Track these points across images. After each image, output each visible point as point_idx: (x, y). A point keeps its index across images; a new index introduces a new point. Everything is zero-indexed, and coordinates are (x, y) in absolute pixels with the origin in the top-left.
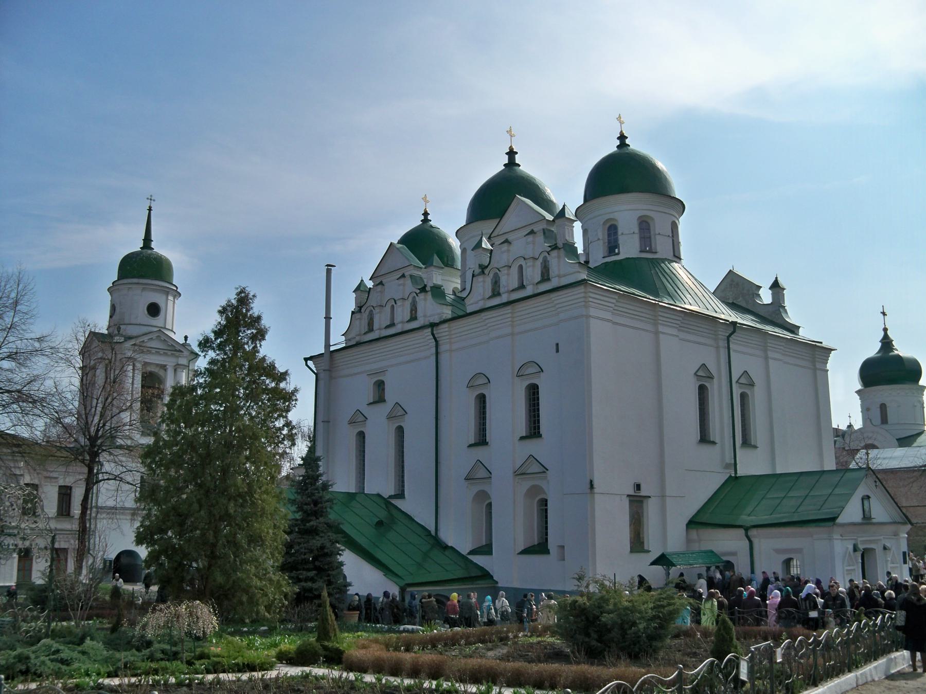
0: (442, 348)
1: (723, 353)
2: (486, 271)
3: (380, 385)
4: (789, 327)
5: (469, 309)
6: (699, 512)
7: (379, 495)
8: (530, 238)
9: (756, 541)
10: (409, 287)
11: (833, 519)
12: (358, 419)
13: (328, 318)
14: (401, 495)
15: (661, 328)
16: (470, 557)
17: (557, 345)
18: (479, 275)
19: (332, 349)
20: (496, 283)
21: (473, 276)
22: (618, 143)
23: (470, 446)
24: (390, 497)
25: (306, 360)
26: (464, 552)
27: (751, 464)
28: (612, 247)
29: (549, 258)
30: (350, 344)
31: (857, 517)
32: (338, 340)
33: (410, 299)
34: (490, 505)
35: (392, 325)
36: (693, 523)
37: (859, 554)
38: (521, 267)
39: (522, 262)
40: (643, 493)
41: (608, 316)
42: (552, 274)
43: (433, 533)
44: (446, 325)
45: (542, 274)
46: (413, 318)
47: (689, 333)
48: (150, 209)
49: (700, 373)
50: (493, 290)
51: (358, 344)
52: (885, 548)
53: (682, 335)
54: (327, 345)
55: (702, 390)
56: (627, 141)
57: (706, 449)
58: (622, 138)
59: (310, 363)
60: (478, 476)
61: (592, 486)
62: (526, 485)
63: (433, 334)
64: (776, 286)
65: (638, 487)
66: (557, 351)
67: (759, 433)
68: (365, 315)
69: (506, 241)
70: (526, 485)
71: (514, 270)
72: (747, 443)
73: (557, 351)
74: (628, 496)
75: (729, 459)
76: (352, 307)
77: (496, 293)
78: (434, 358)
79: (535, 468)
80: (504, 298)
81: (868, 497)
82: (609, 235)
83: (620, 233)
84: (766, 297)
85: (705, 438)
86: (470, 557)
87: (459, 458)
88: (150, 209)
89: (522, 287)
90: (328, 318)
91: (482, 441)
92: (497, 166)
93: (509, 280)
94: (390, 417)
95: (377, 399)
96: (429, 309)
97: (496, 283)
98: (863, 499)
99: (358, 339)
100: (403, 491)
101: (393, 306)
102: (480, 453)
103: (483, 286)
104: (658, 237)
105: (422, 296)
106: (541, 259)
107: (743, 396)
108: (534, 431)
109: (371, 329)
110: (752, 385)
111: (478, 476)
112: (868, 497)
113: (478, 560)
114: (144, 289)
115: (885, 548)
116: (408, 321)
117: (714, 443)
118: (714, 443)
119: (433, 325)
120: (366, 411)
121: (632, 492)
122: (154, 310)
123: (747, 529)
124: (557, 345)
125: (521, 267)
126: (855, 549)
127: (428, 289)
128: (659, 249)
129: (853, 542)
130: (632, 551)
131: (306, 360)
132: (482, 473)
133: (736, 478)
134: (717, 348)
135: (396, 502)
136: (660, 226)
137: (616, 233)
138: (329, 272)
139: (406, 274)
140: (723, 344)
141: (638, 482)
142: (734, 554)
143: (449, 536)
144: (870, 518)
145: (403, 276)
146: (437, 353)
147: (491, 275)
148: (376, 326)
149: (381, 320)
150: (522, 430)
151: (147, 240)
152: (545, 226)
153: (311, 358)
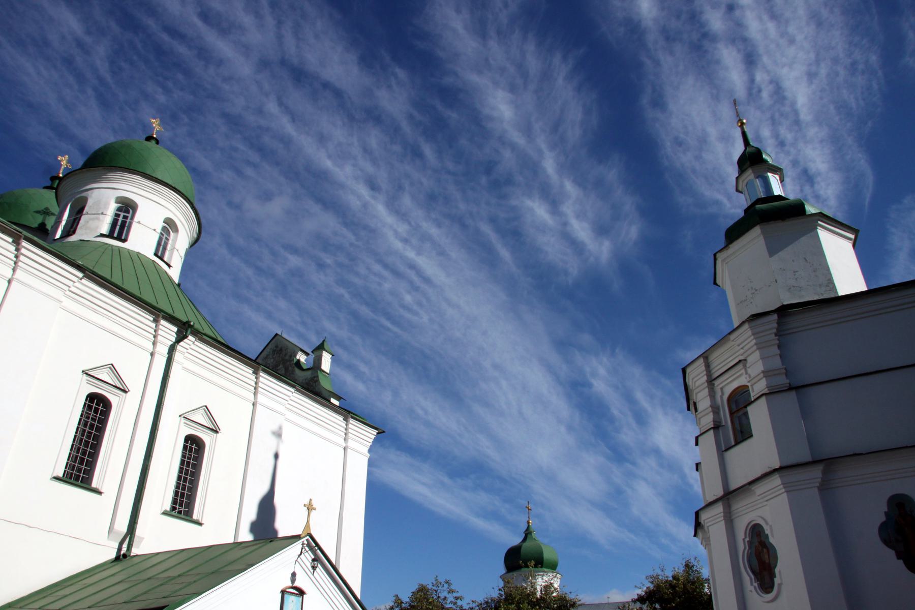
4: (325, 394)
28: (71, 229)
47: (88, 307)
49: (105, 375)
53: (67, 303)
75: (122, 526)
98: (283, 592)
112: (301, 593)
117: (97, 492)
118: (97, 492)
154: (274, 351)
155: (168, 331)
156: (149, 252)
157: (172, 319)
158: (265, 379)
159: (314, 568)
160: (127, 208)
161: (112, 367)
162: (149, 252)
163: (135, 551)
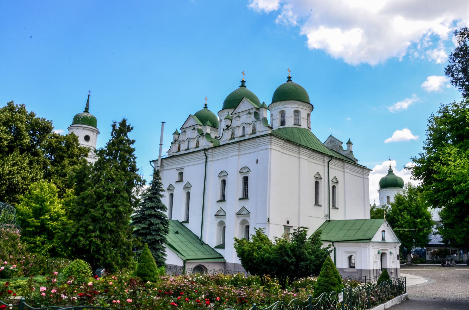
0: (208, 160)
1: (326, 168)
2: (229, 128)
3: (181, 174)
5: (221, 144)
7: (177, 221)
8: (249, 115)
10: (196, 133)
11: (370, 239)
12: (171, 188)
13: (161, 145)
14: (187, 222)
15: (301, 156)
16: (215, 249)
17: (257, 160)
18: (226, 129)
19: (162, 158)
20: (233, 133)
21: (224, 130)
22: (287, 80)
23: (218, 201)
24: (183, 222)
25: (150, 162)
26: (213, 247)
27: (336, 216)
28: (283, 123)
29: (256, 124)
30: (170, 156)
31: (380, 240)
32: (165, 154)
33: (196, 138)
34: (225, 227)
35: (188, 149)
37: (380, 255)
38: (244, 127)
39: (245, 125)
40: (290, 225)
41: (279, 149)
42: (257, 130)
43: (200, 238)
44: (211, 150)
45: (253, 131)
46: (197, 147)
48: (89, 96)
49: (317, 176)
50: (232, 137)
51: (173, 156)
52: (390, 253)
54: (160, 156)
55: (317, 183)
56: (291, 79)
57: (317, 208)
58: (289, 78)
59: (152, 163)
60: (220, 215)
61: (268, 220)
62: (241, 219)
63: (205, 153)
64: (349, 143)
65: (288, 222)
66: (257, 163)
67: (339, 203)
68: (177, 145)
69: (239, 116)
70: (241, 219)
71: (241, 129)
72: (334, 207)
73: (257, 163)
75: (327, 213)
76: (172, 140)
77: (233, 138)
78: (205, 163)
79: (245, 212)
80: (236, 140)
81: (384, 231)
82: (281, 117)
83: (286, 116)
84: (345, 147)
85: (317, 203)
86: (215, 249)
87: (212, 207)
88: (89, 96)
89: (244, 135)
90: (161, 145)
91: (223, 200)
92: (236, 86)
93: (238, 133)
94: (185, 188)
95: (179, 180)
96: (204, 143)
97: (233, 133)
99: (173, 154)
100: (188, 220)
101: (189, 141)
102: (222, 205)
103: (228, 135)
104: (302, 119)
105: (201, 137)
106: (252, 124)
107: (334, 187)
108: (245, 197)
109: (179, 150)
110: (337, 183)
111: (220, 215)
112: (384, 231)
113: (219, 251)
114: (83, 129)
115: (390, 253)
116: (195, 148)
117: (321, 206)
118: (321, 206)
119: (205, 150)
120: (174, 184)
121: (286, 224)
122: (87, 138)
123: (333, 242)
124: (257, 160)
125: (244, 127)
127: (204, 134)
128: (302, 124)
129: (377, 250)
131: (150, 162)
132: (222, 213)
133: (329, 221)
134: (324, 166)
135: (185, 224)
136: (304, 113)
137: (284, 116)
138: (163, 125)
139: (196, 128)
140: (326, 164)
143: (206, 240)
144: (385, 240)
145: (194, 129)
146: (206, 162)
147: (231, 130)
148: (181, 150)
149: (184, 147)
150: (241, 196)
151: (87, 110)
152: (255, 111)
153: (153, 161)
154: (330, 142)
155: (327, 159)
156: (307, 128)
157: (328, 156)
158: (346, 165)
160: (297, 112)
161: (318, 173)
162: (307, 128)
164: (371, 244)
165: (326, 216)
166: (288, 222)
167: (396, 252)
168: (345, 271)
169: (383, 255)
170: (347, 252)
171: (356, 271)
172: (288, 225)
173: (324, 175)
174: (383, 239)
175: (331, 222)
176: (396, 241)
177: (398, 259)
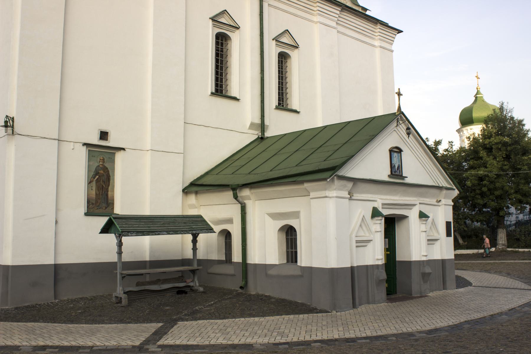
6: (207, 173)
9: (249, 204)
11: (334, 169)
27: (280, 125)
31: (384, 174)
36: (196, 187)
40: (112, 142)
52: (423, 216)
65: (104, 135)
72: (282, 103)
74: (85, 144)
81: (399, 150)
85: (220, 89)
98: (391, 151)
112: (399, 150)
115: (423, 216)
121: (95, 140)
126: (376, 213)
129: (370, 206)
130: (86, 214)
141: (104, 129)
142: (230, 221)
144: (402, 177)
159: (408, 134)
163: (268, 134)
164: (337, 182)
165: (252, 126)
166: (104, 135)
167: (443, 213)
168: (271, 272)
169: (391, 223)
170: (275, 216)
171: (299, 273)
172: (103, 143)
173: (246, 18)
174: (396, 172)
175: (265, 142)
176: (445, 184)
177: (448, 234)
